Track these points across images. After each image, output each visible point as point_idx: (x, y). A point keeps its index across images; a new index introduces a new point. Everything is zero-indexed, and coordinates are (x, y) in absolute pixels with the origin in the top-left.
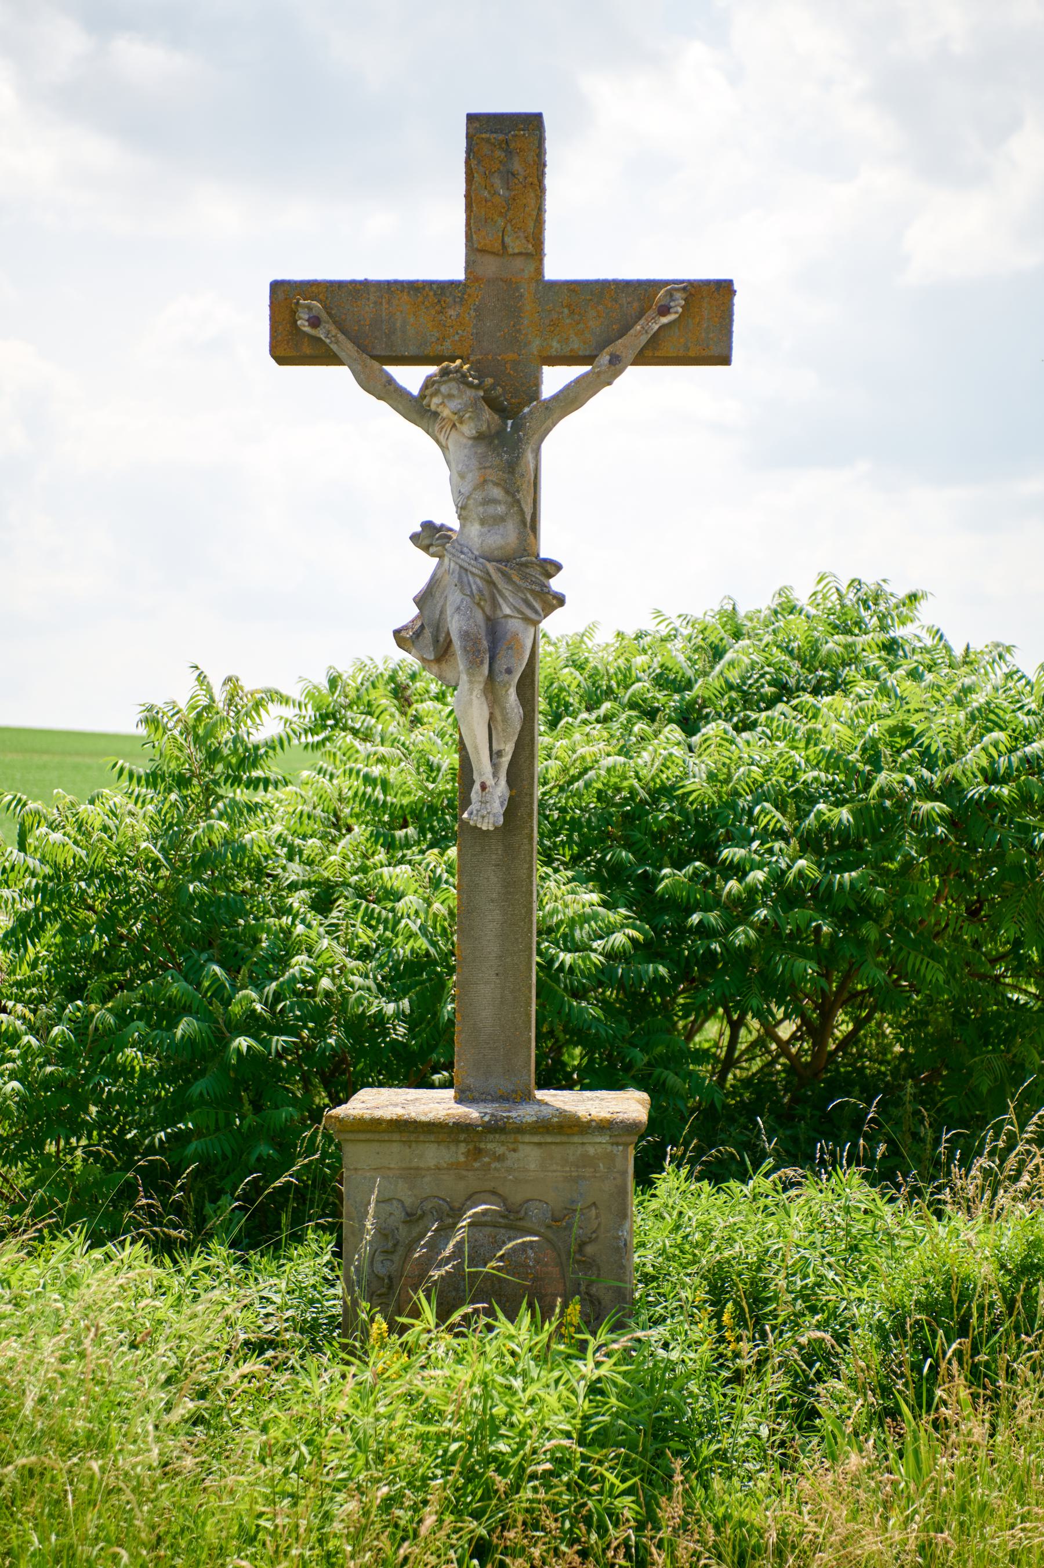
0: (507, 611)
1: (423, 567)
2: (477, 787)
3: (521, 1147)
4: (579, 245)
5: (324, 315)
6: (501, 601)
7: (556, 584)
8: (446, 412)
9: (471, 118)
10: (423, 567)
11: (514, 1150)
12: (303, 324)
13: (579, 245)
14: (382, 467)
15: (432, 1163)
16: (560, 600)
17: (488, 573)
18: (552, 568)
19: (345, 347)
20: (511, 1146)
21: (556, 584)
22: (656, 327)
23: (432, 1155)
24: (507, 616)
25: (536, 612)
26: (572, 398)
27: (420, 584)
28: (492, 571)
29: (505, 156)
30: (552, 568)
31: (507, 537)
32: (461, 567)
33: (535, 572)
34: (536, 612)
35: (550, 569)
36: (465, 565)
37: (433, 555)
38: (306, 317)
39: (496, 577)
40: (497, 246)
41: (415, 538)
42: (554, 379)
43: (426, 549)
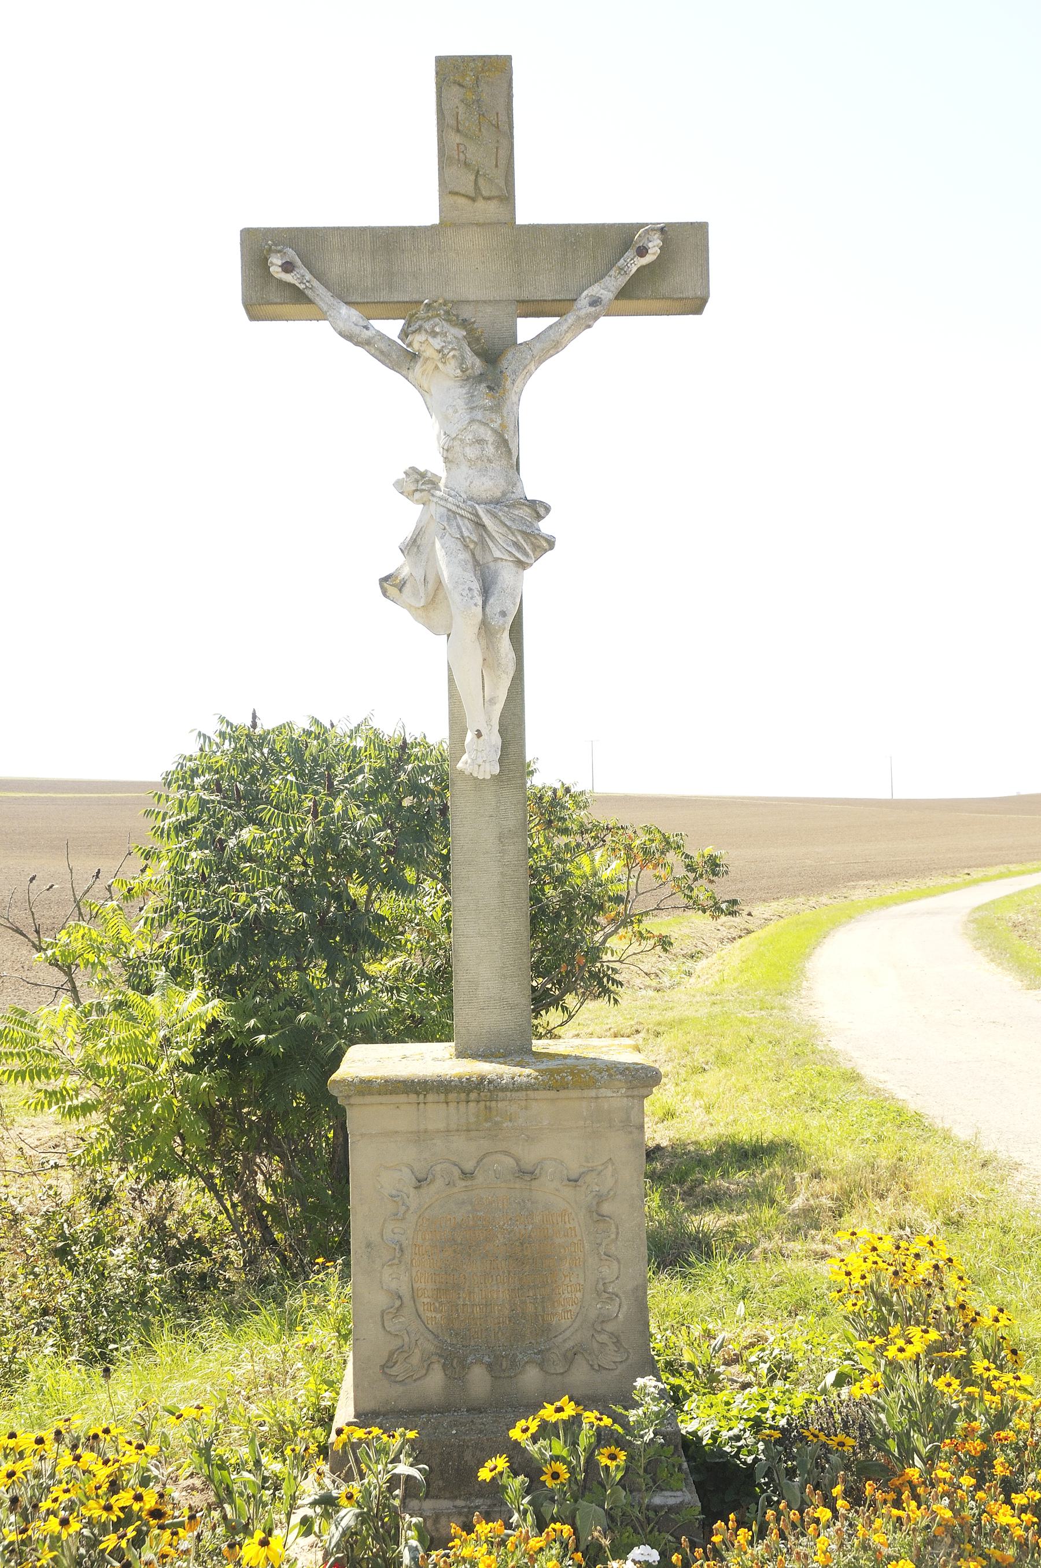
0: (497, 554)
1: (408, 515)
2: (470, 736)
3: (534, 1104)
4: (549, 191)
5: (298, 261)
6: (491, 544)
7: (545, 526)
8: (429, 352)
9: (441, 61)
10: (408, 515)
11: (526, 1108)
12: (276, 271)
13: (549, 191)
14: (363, 412)
15: (441, 1126)
16: (551, 543)
17: (477, 515)
18: (538, 509)
19: (321, 294)
20: (523, 1103)
21: (545, 526)
22: (634, 269)
23: (437, 1115)
24: (496, 560)
25: (526, 554)
26: (549, 345)
27: (407, 532)
28: (481, 513)
29: (475, 97)
30: (538, 509)
31: (487, 485)
32: (449, 510)
33: (524, 512)
34: (526, 554)
35: (542, 511)
36: (454, 508)
37: (417, 502)
38: (280, 263)
39: (486, 520)
40: (470, 190)
41: (399, 485)
42: (528, 328)
43: (410, 495)
